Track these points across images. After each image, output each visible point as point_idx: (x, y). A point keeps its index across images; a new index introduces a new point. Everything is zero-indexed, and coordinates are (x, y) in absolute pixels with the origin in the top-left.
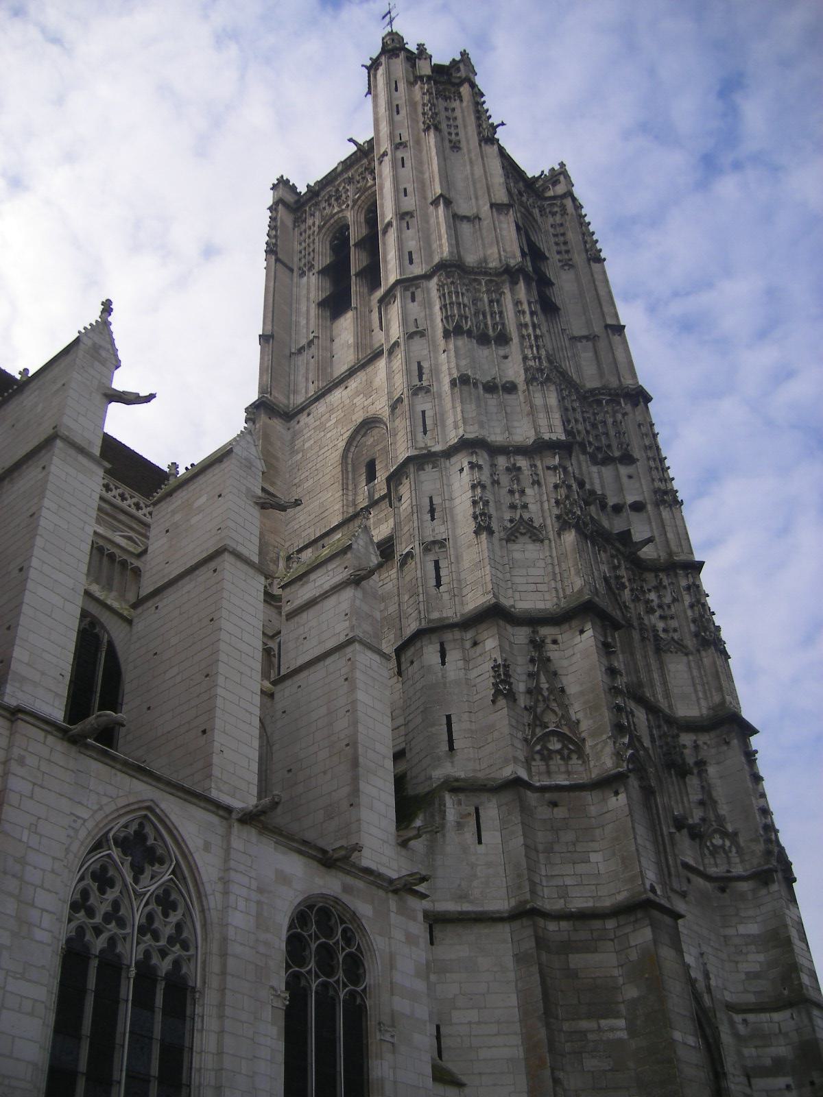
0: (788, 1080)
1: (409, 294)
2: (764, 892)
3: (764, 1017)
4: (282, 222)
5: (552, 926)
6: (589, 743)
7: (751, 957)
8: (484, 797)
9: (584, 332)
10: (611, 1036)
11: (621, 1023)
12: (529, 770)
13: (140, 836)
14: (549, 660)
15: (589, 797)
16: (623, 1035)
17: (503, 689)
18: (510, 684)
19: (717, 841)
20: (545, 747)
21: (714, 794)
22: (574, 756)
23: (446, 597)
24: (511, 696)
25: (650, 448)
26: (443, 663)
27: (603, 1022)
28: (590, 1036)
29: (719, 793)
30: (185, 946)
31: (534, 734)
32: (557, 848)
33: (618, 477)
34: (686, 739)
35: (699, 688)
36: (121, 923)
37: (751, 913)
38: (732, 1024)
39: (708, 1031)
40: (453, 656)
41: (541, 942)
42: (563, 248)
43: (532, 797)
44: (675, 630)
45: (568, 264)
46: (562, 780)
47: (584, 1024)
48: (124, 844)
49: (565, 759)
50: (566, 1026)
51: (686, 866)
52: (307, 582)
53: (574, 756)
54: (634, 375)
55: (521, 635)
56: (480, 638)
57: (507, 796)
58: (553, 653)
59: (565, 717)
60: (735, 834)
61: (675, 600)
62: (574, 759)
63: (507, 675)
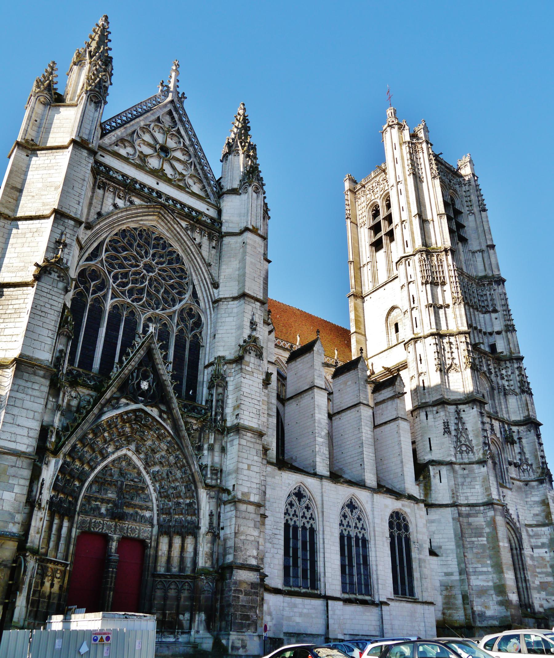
0: (547, 550)
1: (407, 262)
2: (541, 486)
3: (539, 529)
4: (351, 201)
5: (463, 509)
6: (475, 448)
7: (536, 508)
8: (442, 467)
9: (478, 248)
10: (482, 543)
11: (485, 539)
12: (456, 458)
13: (351, 502)
14: (462, 418)
15: (475, 466)
16: (485, 542)
17: (447, 430)
18: (449, 428)
19: (525, 467)
20: (460, 449)
21: (525, 450)
22: (470, 452)
23: (427, 394)
24: (449, 432)
25: (505, 305)
26: (427, 419)
27: (479, 539)
28: (475, 543)
29: (526, 450)
30: (365, 530)
31: (457, 445)
32: (465, 484)
33: (491, 319)
34: (514, 429)
35: (520, 409)
36: (350, 527)
37: (536, 493)
38: (527, 531)
39: (518, 535)
40: (430, 416)
41: (460, 514)
42: (469, 204)
43: (457, 467)
44: (512, 386)
45: (471, 212)
46: (466, 461)
47: (474, 539)
48: (348, 506)
49: (468, 453)
50: (468, 540)
51: (512, 478)
52: (381, 394)
53: (470, 452)
54: (499, 270)
55: (452, 408)
56: (439, 411)
57: (448, 467)
58: (463, 415)
59: (468, 438)
60: (531, 465)
61: (512, 373)
62: (471, 454)
63: (448, 425)
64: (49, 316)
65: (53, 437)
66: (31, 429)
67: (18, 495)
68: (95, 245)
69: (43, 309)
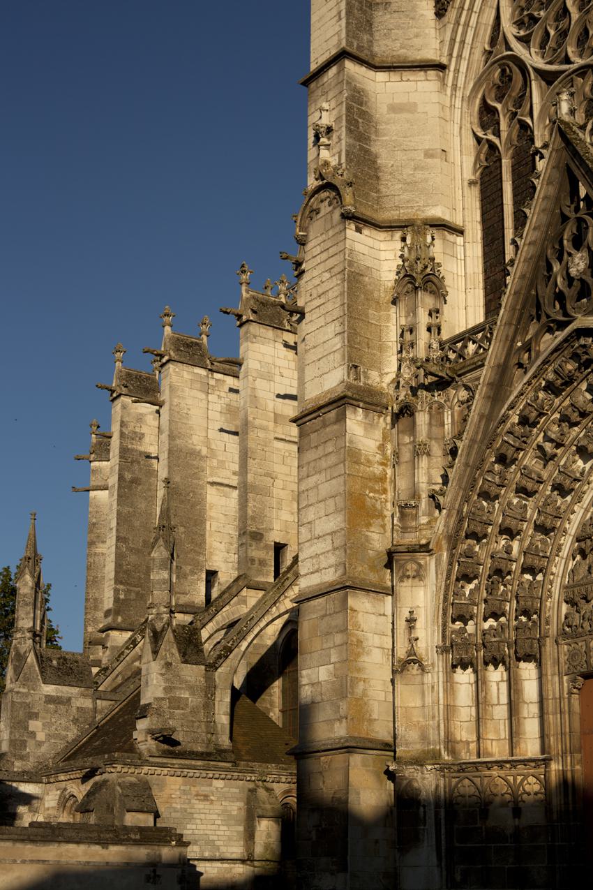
64: (331, 294)
65: (420, 513)
66: (335, 532)
67: (337, 665)
68: (489, 17)
69: (321, 290)
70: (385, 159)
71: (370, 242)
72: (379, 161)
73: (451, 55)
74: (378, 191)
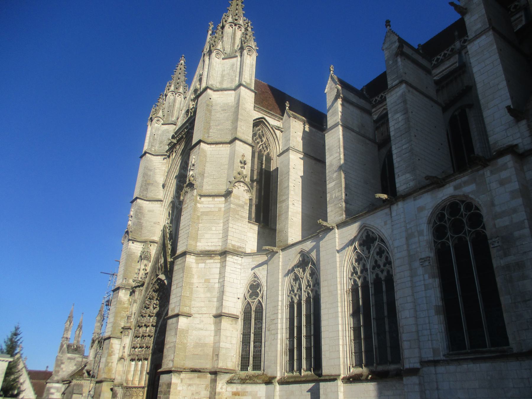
70: (144, 224)
71: (136, 246)
72: (143, 224)
73: (164, 198)
74: (141, 232)
